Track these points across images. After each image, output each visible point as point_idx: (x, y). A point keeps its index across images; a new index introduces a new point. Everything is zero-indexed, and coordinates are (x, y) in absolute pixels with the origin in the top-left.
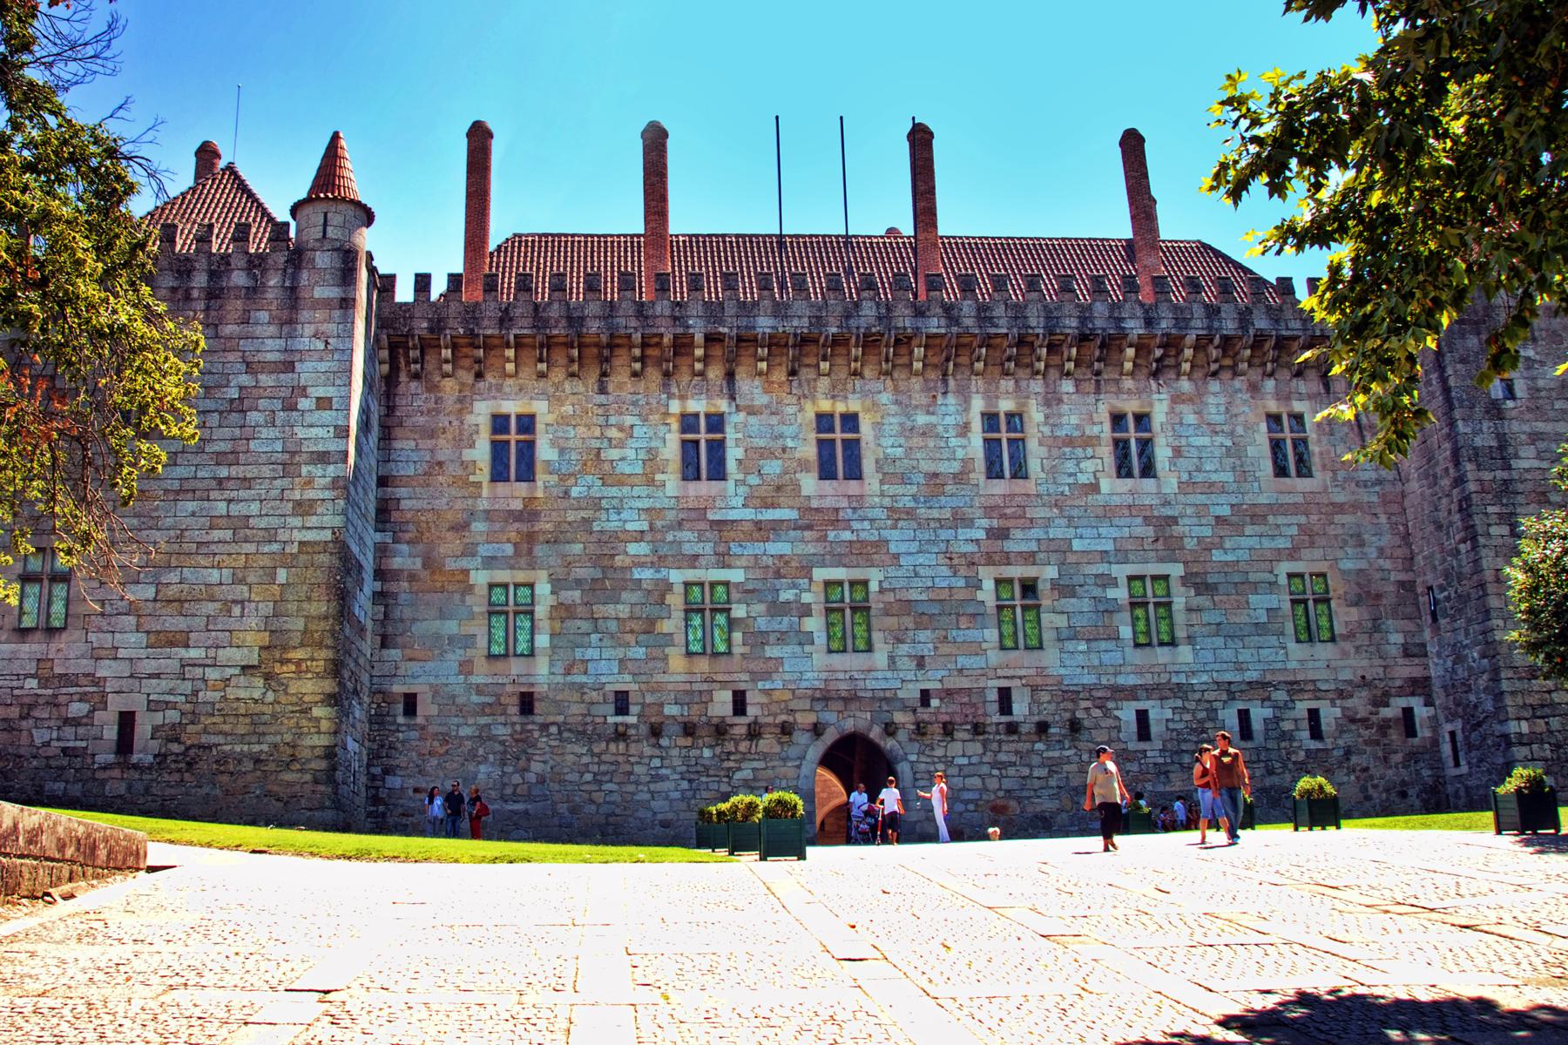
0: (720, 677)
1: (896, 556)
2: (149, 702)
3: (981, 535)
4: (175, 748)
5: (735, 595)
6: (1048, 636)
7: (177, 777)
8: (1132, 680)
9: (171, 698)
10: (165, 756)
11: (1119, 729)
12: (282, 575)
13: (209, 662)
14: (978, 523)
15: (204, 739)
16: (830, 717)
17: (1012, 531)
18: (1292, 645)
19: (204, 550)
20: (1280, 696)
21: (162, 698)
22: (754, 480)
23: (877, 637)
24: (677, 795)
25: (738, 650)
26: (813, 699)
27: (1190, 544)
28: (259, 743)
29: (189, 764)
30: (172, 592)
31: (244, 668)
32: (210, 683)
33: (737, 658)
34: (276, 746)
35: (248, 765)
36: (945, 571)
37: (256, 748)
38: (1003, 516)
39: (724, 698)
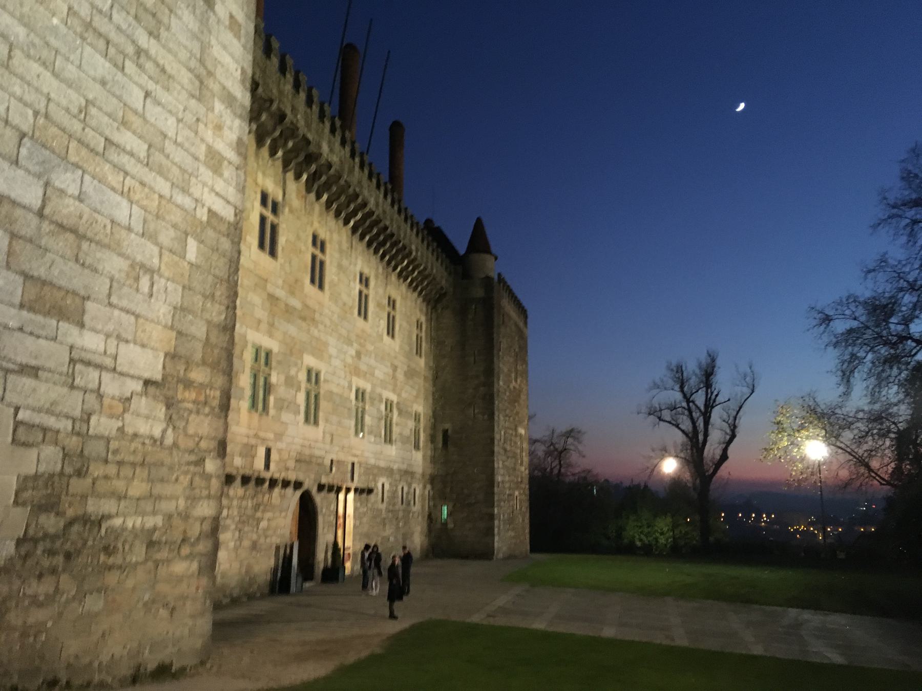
0: (262, 434)
1: (330, 357)
2: (17, 424)
3: (354, 353)
4: (50, 523)
5: (274, 364)
6: (366, 429)
7: (43, 588)
8: (382, 464)
9: (51, 422)
10: (35, 541)
11: (377, 494)
12: (192, 249)
13: (108, 362)
14: (355, 345)
15: (93, 507)
16: (301, 478)
17: (362, 356)
18: (414, 452)
19: (113, 155)
20: (409, 479)
21: (37, 419)
22: (287, 268)
23: (321, 415)
24: (232, 544)
25: (272, 412)
26: (297, 461)
27: (399, 384)
28: (154, 513)
29: (68, 556)
30: (67, 208)
31: (147, 383)
32: (106, 401)
33: (270, 417)
34: (169, 517)
35: (138, 553)
36: (342, 374)
37: (150, 522)
38: (360, 344)
39: (261, 452)
